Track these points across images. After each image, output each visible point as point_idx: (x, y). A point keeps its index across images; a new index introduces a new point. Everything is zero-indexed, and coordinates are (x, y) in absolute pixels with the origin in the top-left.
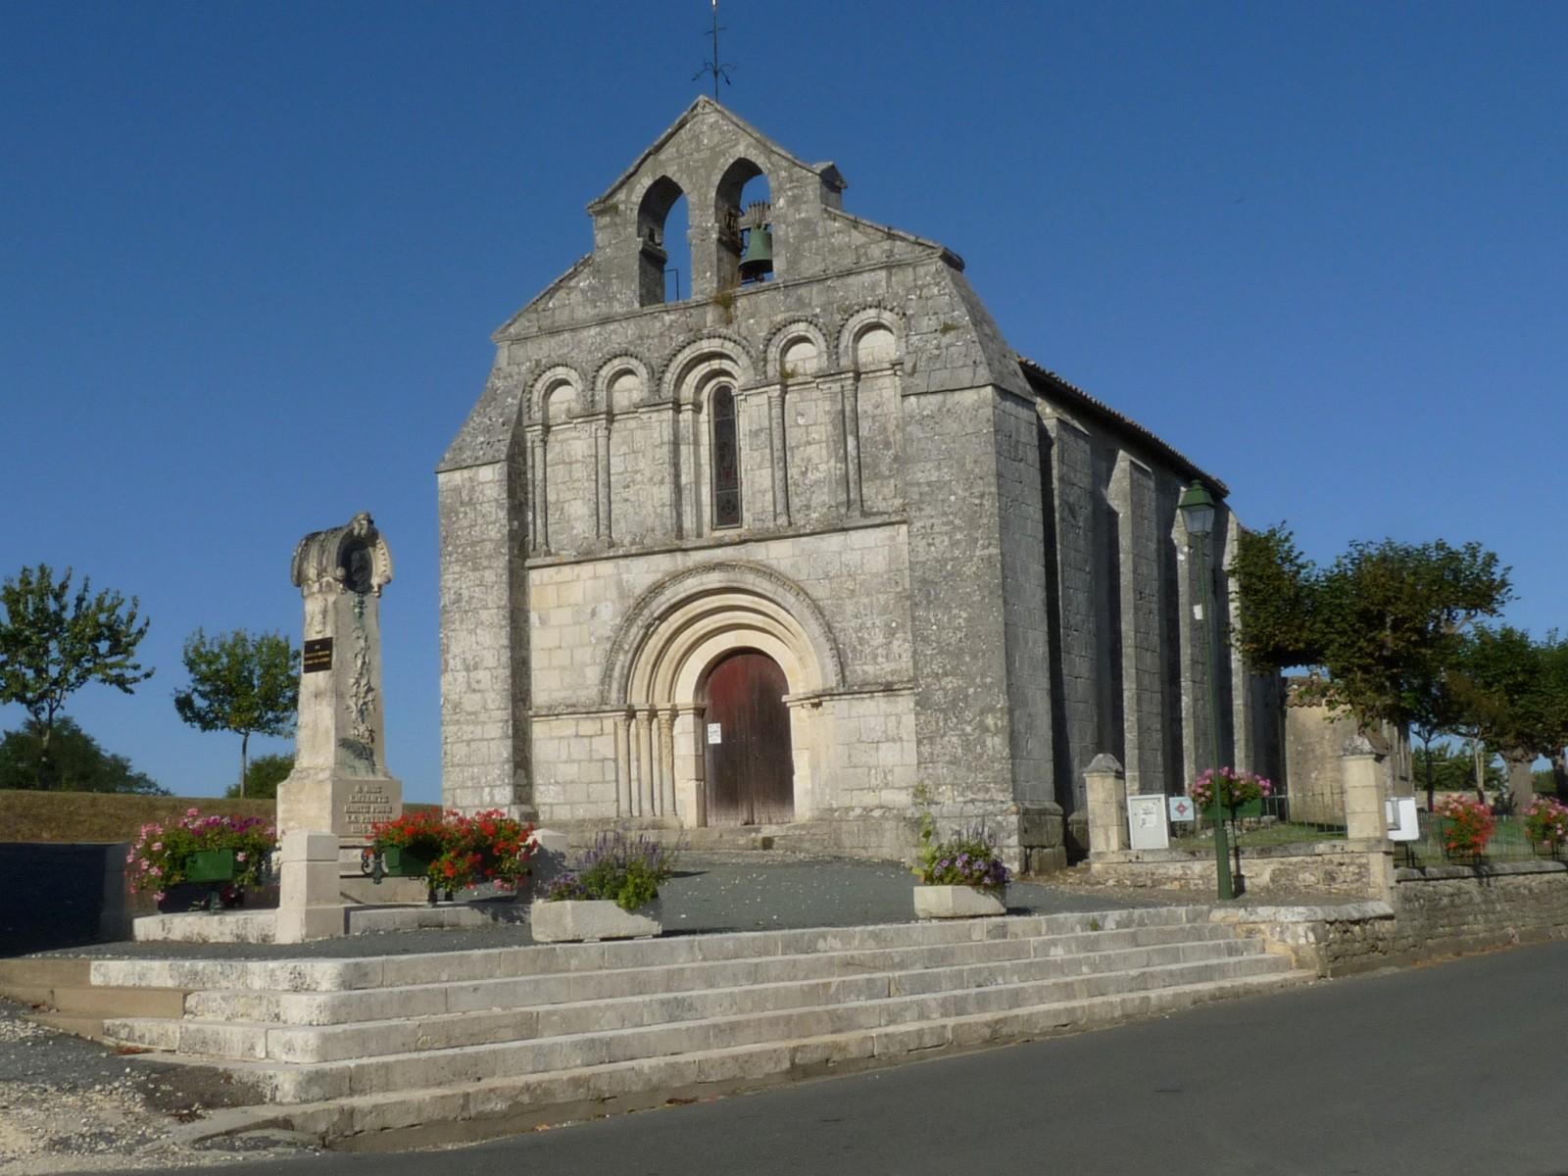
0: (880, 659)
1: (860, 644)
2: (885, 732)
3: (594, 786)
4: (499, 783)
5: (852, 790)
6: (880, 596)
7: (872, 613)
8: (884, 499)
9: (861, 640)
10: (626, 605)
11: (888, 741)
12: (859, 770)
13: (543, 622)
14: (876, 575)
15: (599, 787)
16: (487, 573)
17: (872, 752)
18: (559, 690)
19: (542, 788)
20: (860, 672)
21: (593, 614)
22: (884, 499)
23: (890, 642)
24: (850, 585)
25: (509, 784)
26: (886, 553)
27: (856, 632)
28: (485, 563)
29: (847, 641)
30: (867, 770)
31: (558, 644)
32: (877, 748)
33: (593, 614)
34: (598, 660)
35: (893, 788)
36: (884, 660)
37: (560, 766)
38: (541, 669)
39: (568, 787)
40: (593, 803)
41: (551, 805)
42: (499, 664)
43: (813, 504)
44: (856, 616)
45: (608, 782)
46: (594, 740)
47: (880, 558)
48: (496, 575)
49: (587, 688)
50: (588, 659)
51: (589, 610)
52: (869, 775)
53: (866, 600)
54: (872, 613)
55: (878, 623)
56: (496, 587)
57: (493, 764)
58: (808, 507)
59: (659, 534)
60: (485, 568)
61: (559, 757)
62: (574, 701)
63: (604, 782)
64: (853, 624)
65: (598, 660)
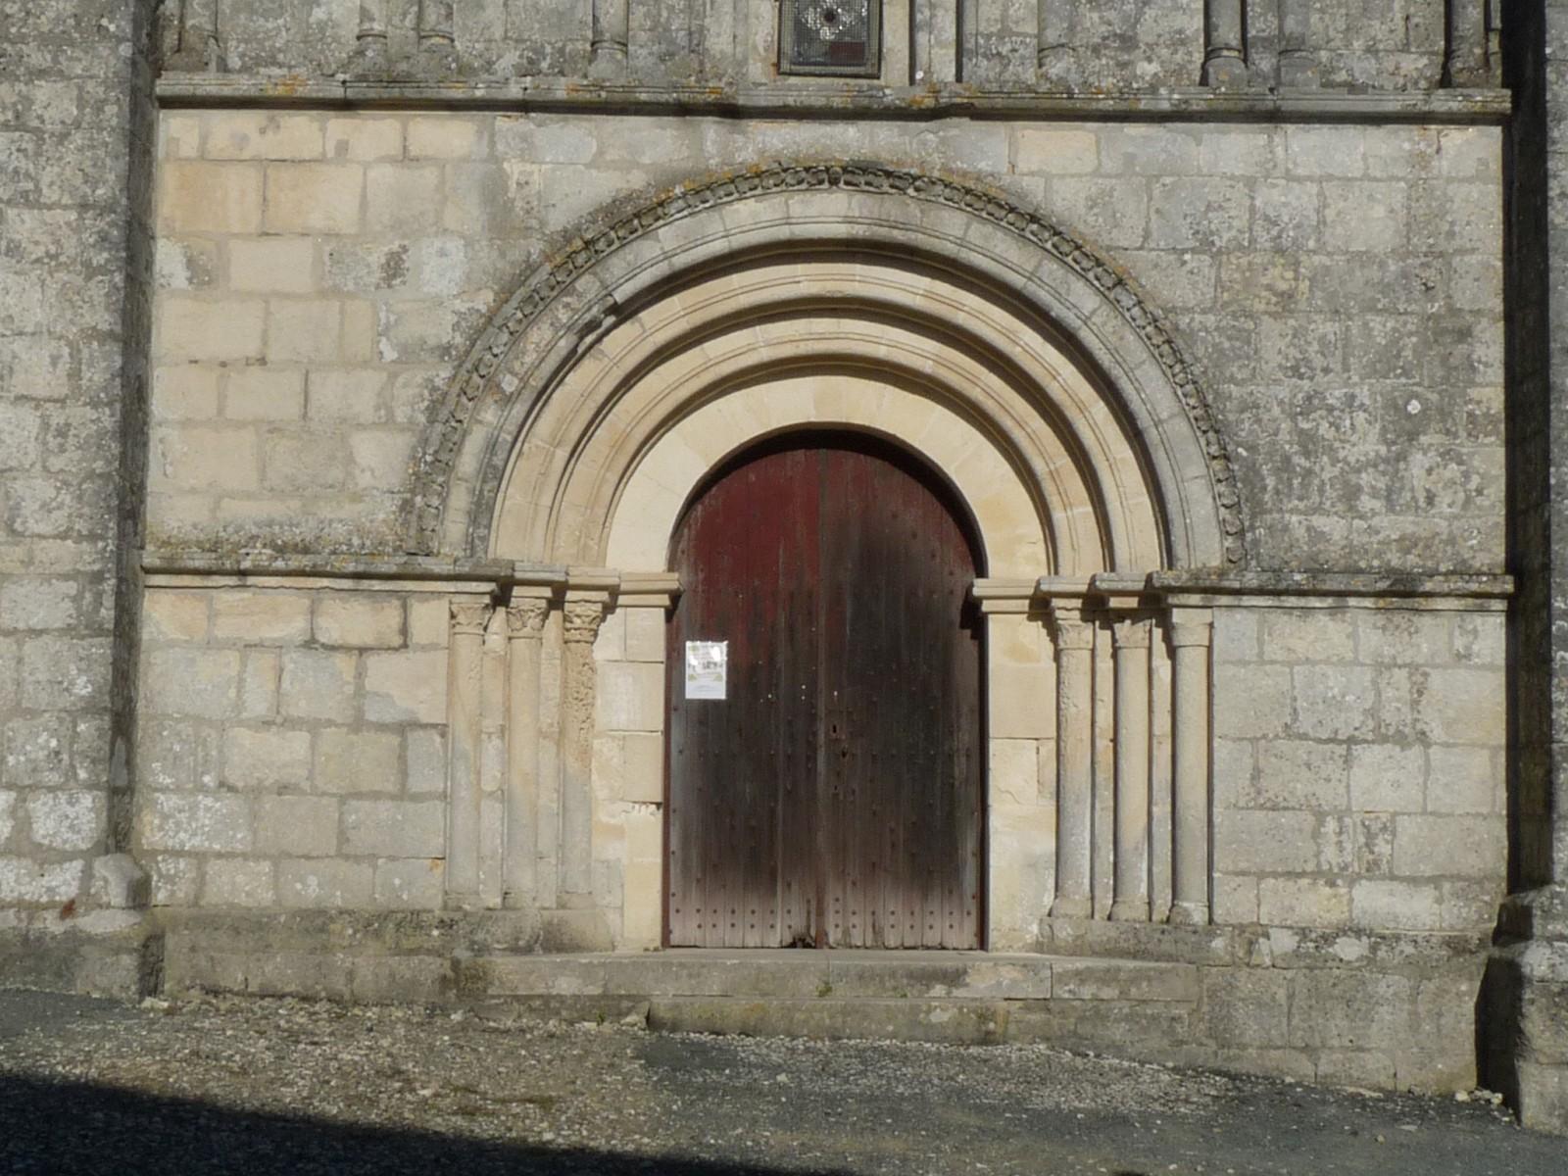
0: (1366, 503)
1: (1307, 454)
2: (1372, 713)
3: (366, 805)
4: (54, 778)
5: (1261, 875)
6: (1375, 322)
7: (1346, 368)
8: (1371, 50)
9: (1308, 443)
10: (516, 255)
11: (1384, 739)
12: (1285, 819)
13: (203, 275)
14: (1364, 258)
15: (385, 810)
16: (43, 91)
17: (1332, 769)
18: (249, 496)
19: (168, 802)
20: (1300, 533)
21: (394, 268)
22: (1371, 50)
23: (1401, 457)
24: (1279, 277)
25: (90, 786)
26: (1398, 200)
27: (1293, 417)
28: (38, 58)
29: (1263, 440)
30: (1311, 819)
31: (252, 349)
32: (1348, 761)
33: (394, 268)
34: (401, 416)
35: (1393, 878)
36: (1378, 505)
37: (245, 737)
38: (186, 424)
39: (269, 803)
40: (357, 859)
41: (200, 857)
42: (76, 391)
43: (1146, 33)
44: (1295, 369)
45: (416, 798)
46: (372, 661)
47: (1379, 211)
48: (81, 103)
49: (356, 498)
50: (364, 406)
51: (377, 257)
52: (1316, 835)
53: (1329, 328)
54: (1346, 368)
55: (1363, 395)
56: (78, 139)
57: (32, 713)
58: (1128, 42)
59: (643, 54)
60: (42, 73)
61: (239, 706)
62: (305, 531)
63: (402, 795)
64: (1283, 393)
65: (401, 416)
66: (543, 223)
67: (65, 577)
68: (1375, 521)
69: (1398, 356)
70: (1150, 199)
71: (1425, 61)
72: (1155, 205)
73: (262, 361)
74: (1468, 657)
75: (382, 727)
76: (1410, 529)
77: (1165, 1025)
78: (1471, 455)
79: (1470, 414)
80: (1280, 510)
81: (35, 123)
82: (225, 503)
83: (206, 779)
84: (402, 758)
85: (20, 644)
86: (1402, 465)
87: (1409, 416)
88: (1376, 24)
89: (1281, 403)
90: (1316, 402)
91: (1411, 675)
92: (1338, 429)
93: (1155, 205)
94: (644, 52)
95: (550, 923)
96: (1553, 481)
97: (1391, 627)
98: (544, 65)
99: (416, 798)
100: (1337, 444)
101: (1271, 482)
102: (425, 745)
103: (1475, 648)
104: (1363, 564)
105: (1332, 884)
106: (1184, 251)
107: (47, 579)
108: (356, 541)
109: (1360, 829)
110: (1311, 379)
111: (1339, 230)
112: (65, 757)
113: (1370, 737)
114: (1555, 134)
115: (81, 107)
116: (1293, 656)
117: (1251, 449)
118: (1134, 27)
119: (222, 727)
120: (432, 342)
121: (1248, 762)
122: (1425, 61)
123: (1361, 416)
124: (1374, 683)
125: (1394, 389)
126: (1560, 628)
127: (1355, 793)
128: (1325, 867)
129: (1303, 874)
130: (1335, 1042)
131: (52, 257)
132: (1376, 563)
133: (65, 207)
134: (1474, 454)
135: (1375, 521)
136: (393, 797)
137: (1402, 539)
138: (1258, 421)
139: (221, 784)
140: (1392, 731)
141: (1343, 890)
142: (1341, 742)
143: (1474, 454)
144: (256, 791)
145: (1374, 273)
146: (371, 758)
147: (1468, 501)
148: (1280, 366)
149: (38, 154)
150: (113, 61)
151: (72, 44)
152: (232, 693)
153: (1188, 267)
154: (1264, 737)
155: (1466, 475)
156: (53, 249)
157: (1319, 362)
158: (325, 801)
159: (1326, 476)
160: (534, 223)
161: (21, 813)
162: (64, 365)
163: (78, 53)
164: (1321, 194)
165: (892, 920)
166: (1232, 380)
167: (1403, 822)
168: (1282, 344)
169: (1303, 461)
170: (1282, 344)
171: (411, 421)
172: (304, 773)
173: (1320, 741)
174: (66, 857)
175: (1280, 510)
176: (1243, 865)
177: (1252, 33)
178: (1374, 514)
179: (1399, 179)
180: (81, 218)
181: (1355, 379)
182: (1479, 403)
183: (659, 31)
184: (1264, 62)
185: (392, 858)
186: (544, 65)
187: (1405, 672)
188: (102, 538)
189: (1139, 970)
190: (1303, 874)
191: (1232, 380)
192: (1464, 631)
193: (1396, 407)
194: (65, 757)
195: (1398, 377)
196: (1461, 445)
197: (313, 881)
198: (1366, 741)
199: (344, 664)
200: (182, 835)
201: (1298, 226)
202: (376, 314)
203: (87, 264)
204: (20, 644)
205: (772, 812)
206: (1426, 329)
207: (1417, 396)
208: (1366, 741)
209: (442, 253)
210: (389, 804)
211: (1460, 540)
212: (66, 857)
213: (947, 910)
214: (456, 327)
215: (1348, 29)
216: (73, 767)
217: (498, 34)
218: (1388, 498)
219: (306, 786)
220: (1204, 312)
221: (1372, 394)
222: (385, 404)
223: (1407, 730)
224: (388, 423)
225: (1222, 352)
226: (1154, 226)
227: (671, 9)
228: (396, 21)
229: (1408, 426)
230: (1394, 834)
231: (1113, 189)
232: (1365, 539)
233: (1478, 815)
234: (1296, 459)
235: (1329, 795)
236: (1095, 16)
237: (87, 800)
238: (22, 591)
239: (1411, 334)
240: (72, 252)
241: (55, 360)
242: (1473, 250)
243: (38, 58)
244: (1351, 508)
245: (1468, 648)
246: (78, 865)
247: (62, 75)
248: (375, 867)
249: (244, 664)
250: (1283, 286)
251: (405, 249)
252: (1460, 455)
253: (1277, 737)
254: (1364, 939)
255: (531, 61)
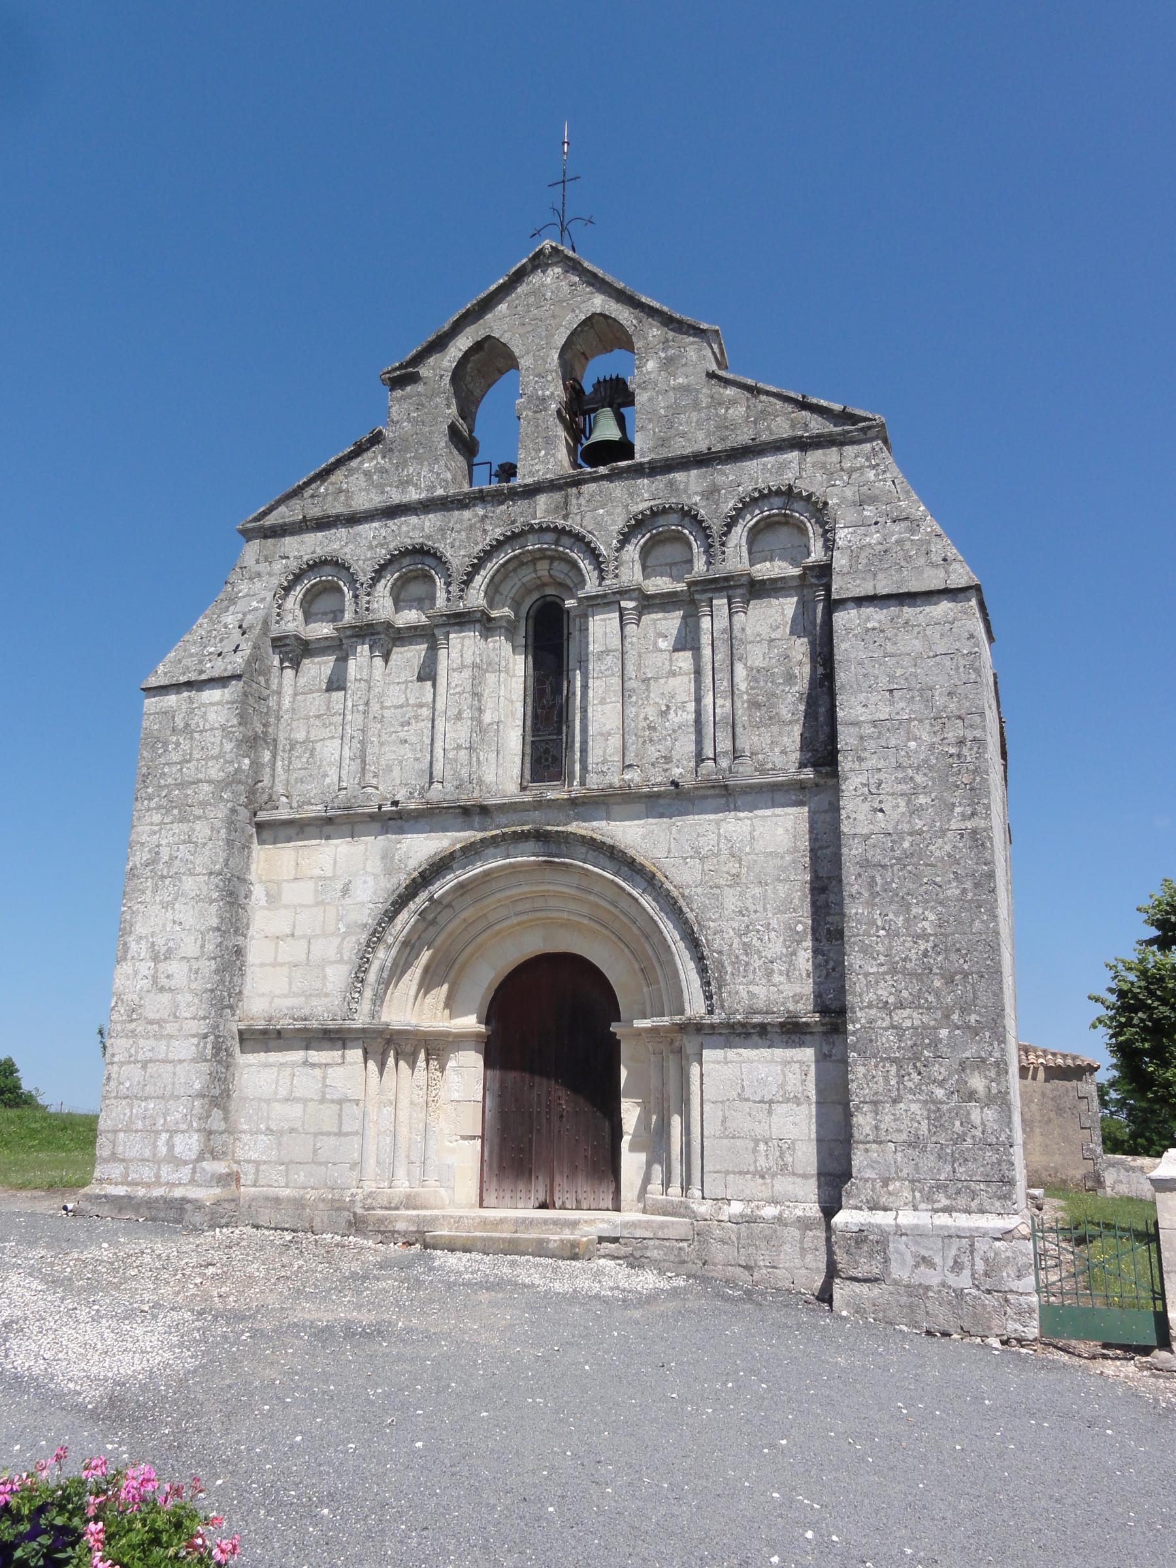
0: (777, 978)
1: (747, 954)
2: (782, 1086)
3: (325, 1138)
4: (183, 1127)
5: (727, 1173)
6: (780, 887)
7: (765, 910)
8: (783, 752)
9: (747, 948)
10: (395, 881)
11: (788, 1101)
12: (739, 1142)
13: (273, 899)
14: (773, 855)
15: (332, 1140)
16: (198, 826)
17: (762, 1116)
18: (285, 996)
19: (245, 1137)
20: (744, 995)
21: (346, 891)
22: (783, 752)
23: (794, 953)
24: (733, 867)
25: (199, 1131)
26: (789, 825)
27: (740, 936)
28: (198, 812)
29: (726, 948)
30: (752, 1144)
31: (288, 931)
32: (770, 1112)
33: (346, 891)
34: (346, 958)
35: (794, 1174)
36: (783, 979)
37: (278, 1108)
38: (262, 965)
39: (285, 1139)
40: (320, 1164)
41: (257, 1163)
42: (203, 953)
43: (676, 756)
44: (740, 912)
45: (347, 1134)
46: (330, 1070)
47: (780, 831)
48: (212, 829)
49: (326, 995)
50: (332, 953)
51: (339, 886)
52: (755, 1151)
53: (758, 890)
54: (765, 910)
55: (774, 923)
56: (210, 845)
57: (178, 1098)
58: (668, 759)
59: (449, 787)
60: (198, 818)
61: (276, 1093)
62: (306, 1011)
63: (340, 1134)
64: (735, 925)
65: (346, 958)
66: (406, 866)
67: (194, 1036)
68: (781, 987)
69: (791, 903)
70: (671, 833)
71: (810, 754)
72: (673, 836)
73: (293, 935)
74: (830, 1056)
75: (333, 1101)
76: (798, 990)
77: (676, 1252)
78: (829, 950)
79: (828, 930)
80: (734, 984)
81: (195, 840)
82: (276, 1000)
83: (261, 1126)
84: (340, 1116)
85: (175, 1066)
86: (794, 957)
87: (798, 933)
88: (785, 739)
89: (733, 929)
90: (751, 927)
91: (801, 1066)
92: (762, 940)
93: (673, 836)
94: (450, 785)
95: (410, 1195)
96: (846, 963)
97: (790, 1041)
98: (416, 794)
99: (347, 1134)
100: (761, 949)
101: (729, 969)
102: (350, 1110)
103: (834, 1051)
104: (775, 1009)
105: (763, 1177)
106: (687, 858)
107: (186, 1037)
108: (326, 1015)
109: (777, 1149)
110: (748, 916)
111: (761, 842)
112: (189, 1117)
113: (781, 1099)
114: (844, 787)
115: (212, 831)
116: (741, 1058)
117: (720, 953)
118: (671, 751)
119: (268, 1102)
120: (360, 922)
121: (720, 1114)
122: (810, 754)
123: (774, 933)
124: (782, 1071)
125: (790, 919)
126: (852, 1040)
127: (774, 1130)
128: (759, 1168)
129: (748, 1172)
130: (761, 1263)
131: (198, 896)
132: (782, 1008)
133: (204, 874)
134: (830, 950)
135: (781, 987)
136: (336, 1134)
137: (795, 995)
138: (723, 939)
139: (267, 1129)
140: (792, 1095)
141: (769, 1181)
142: (765, 1103)
143: (830, 950)
144: (281, 1132)
145: (779, 862)
146: (327, 1116)
147: (828, 975)
148: (733, 911)
149: (195, 852)
150: (225, 810)
151: (211, 805)
152: (274, 1086)
153: (689, 865)
154: (728, 1100)
155: (827, 962)
156: (198, 892)
157: (752, 908)
158: (308, 1136)
159: (756, 965)
160: (403, 866)
161: (171, 1143)
162: (199, 943)
163: (213, 809)
164: (752, 825)
165: (585, 1195)
166: (710, 919)
167: (799, 1145)
168: (734, 900)
169: (745, 958)
170: (734, 900)
171: (350, 958)
172: (300, 1124)
173: (755, 1102)
174: (186, 1163)
175: (734, 984)
176: (718, 1168)
177: (718, 750)
178: (781, 983)
179: (790, 815)
180: (209, 878)
181: (770, 915)
182: (832, 924)
183: (456, 775)
184: (724, 763)
185: (334, 1164)
186: (416, 794)
187: (797, 1065)
188: (208, 1018)
189: (663, 1222)
190: (748, 1172)
191: (710, 919)
192: (828, 1043)
193: (791, 930)
194: (189, 1117)
195: (791, 913)
196: (824, 946)
197: (302, 1174)
198: (779, 1102)
199: (317, 1072)
200: (251, 1153)
201: (742, 841)
202: (338, 911)
203: (210, 898)
204: (175, 1066)
205: (531, 1139)
206: (805, 888)
207: (800, 922)
208: (779, 1102)
209: (365, 882)
210: (334, 1138)
211: (824, 995)
212: (186, 1163)
213: (519, 1188)
214: (369, 915)
215: (772, 742)
216: (191, 1121)
217: (398, 782)
218: (788, 975)
219: (301, 1129)
220: (696, 887)
221: (779, 922)
222: (340, 951)
223: (799, 1095)
224: (341, 961)
225: (705, 906)
226: (672, 846)
227: (462, 765)
228: (351, 781)
229: (797, 938)
230: (794, 1150)
231: (653, 830)
232: (776, 996)
233: (837, 1140)
234: (741, 957)
235: (760, 1130)
236: (653, 748)
237: (196, 1136)
238: (177, 1043)
239: (797, 891)
240: (205, 893)
241: (196, 940)
242: (828, 847)
243: (198, 812)
244: (769, 981)
245: (830, 1051)
246: (191, 1166)
247: (207, 819)
248: (327, 1168)
249: (279, 1073)
250: (734, 871)
251: (350, 881)
252: (823, 951)
253: (734, 1100)
254: (778, 1207)
255: (411, 793)
